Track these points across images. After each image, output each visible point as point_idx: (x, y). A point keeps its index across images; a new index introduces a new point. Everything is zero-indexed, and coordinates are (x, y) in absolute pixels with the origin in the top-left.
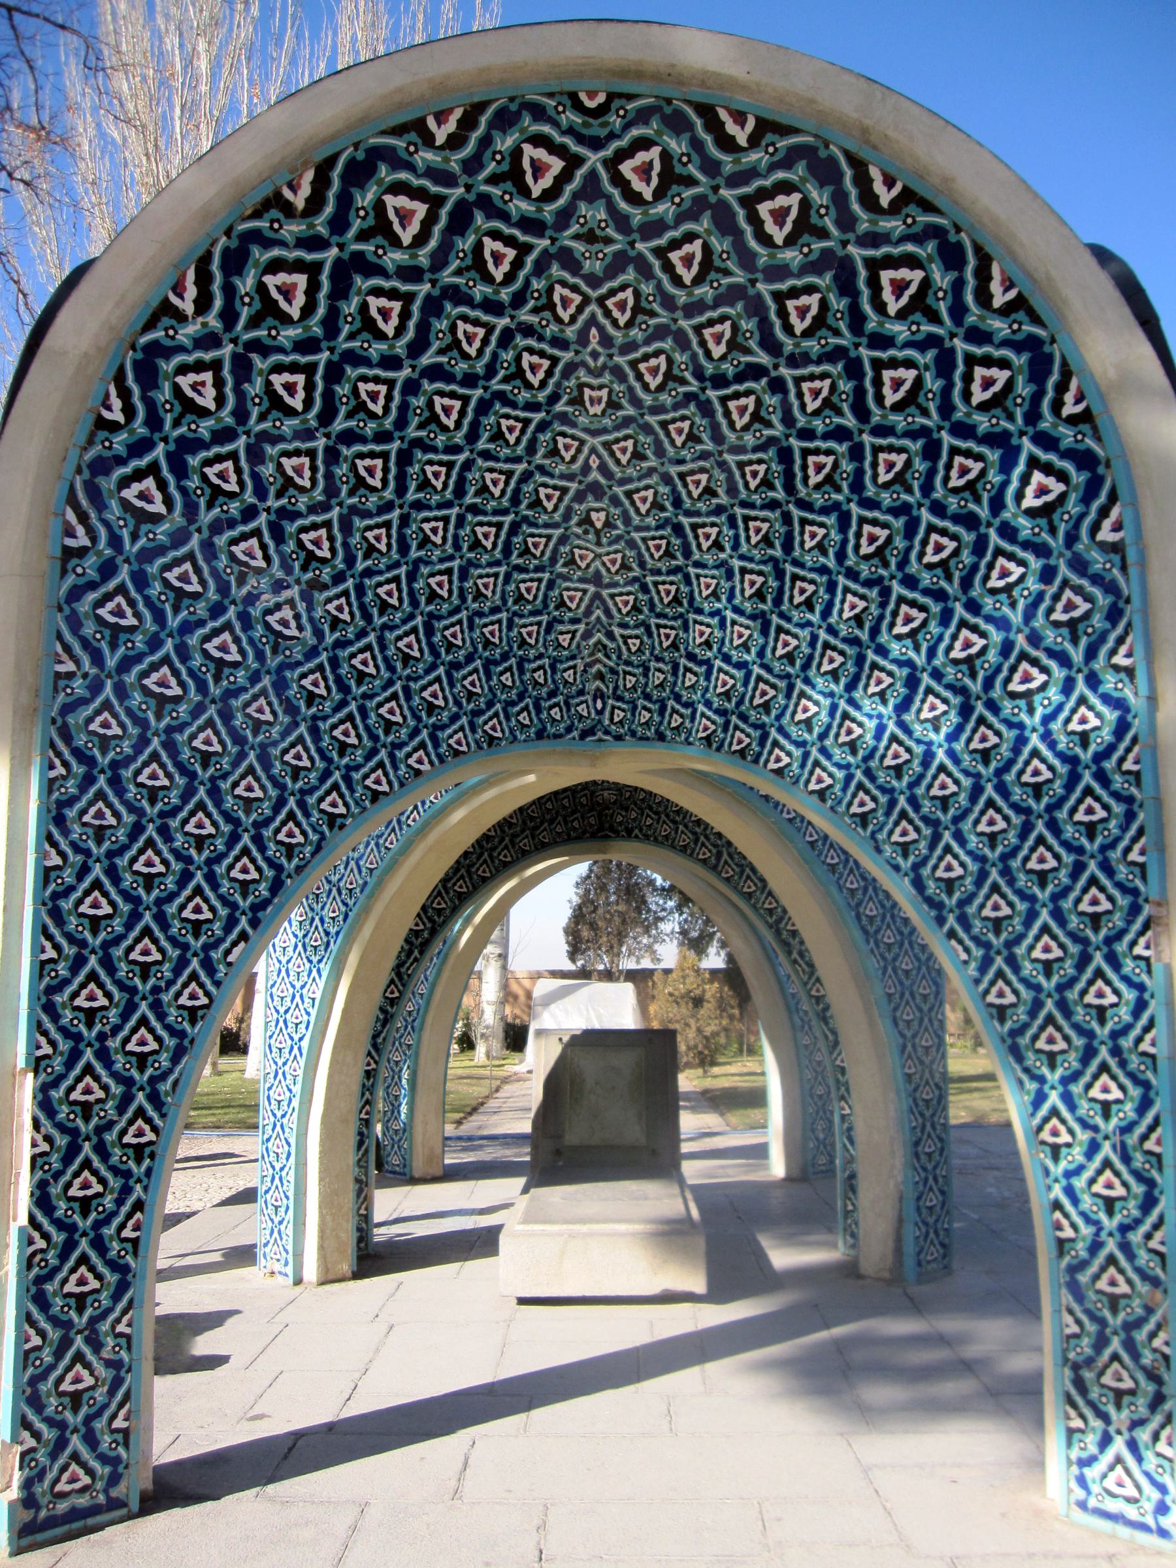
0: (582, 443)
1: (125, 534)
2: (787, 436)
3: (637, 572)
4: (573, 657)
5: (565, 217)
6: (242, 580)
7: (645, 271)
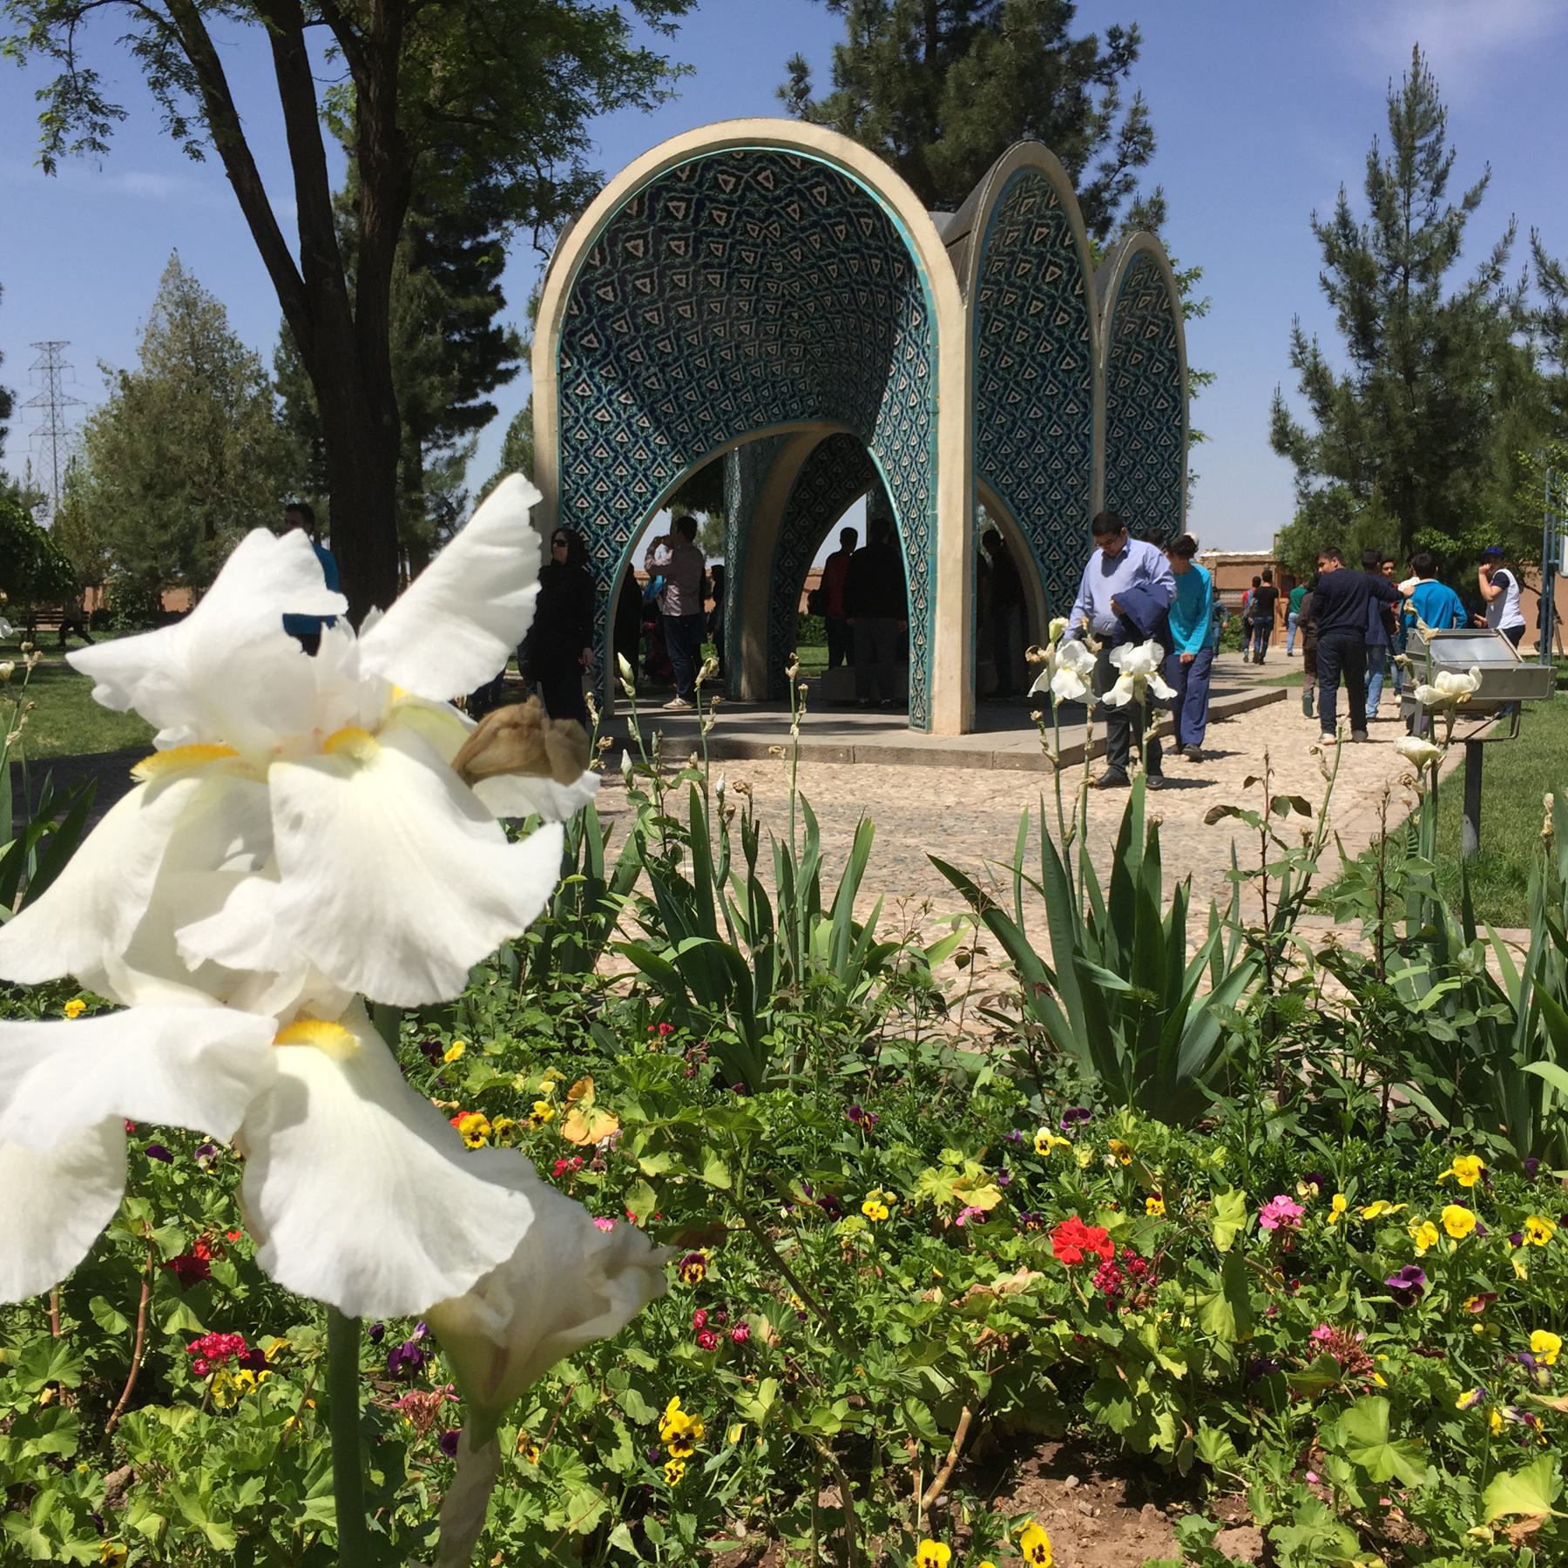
5: (742, 199)
6: (633, 369)
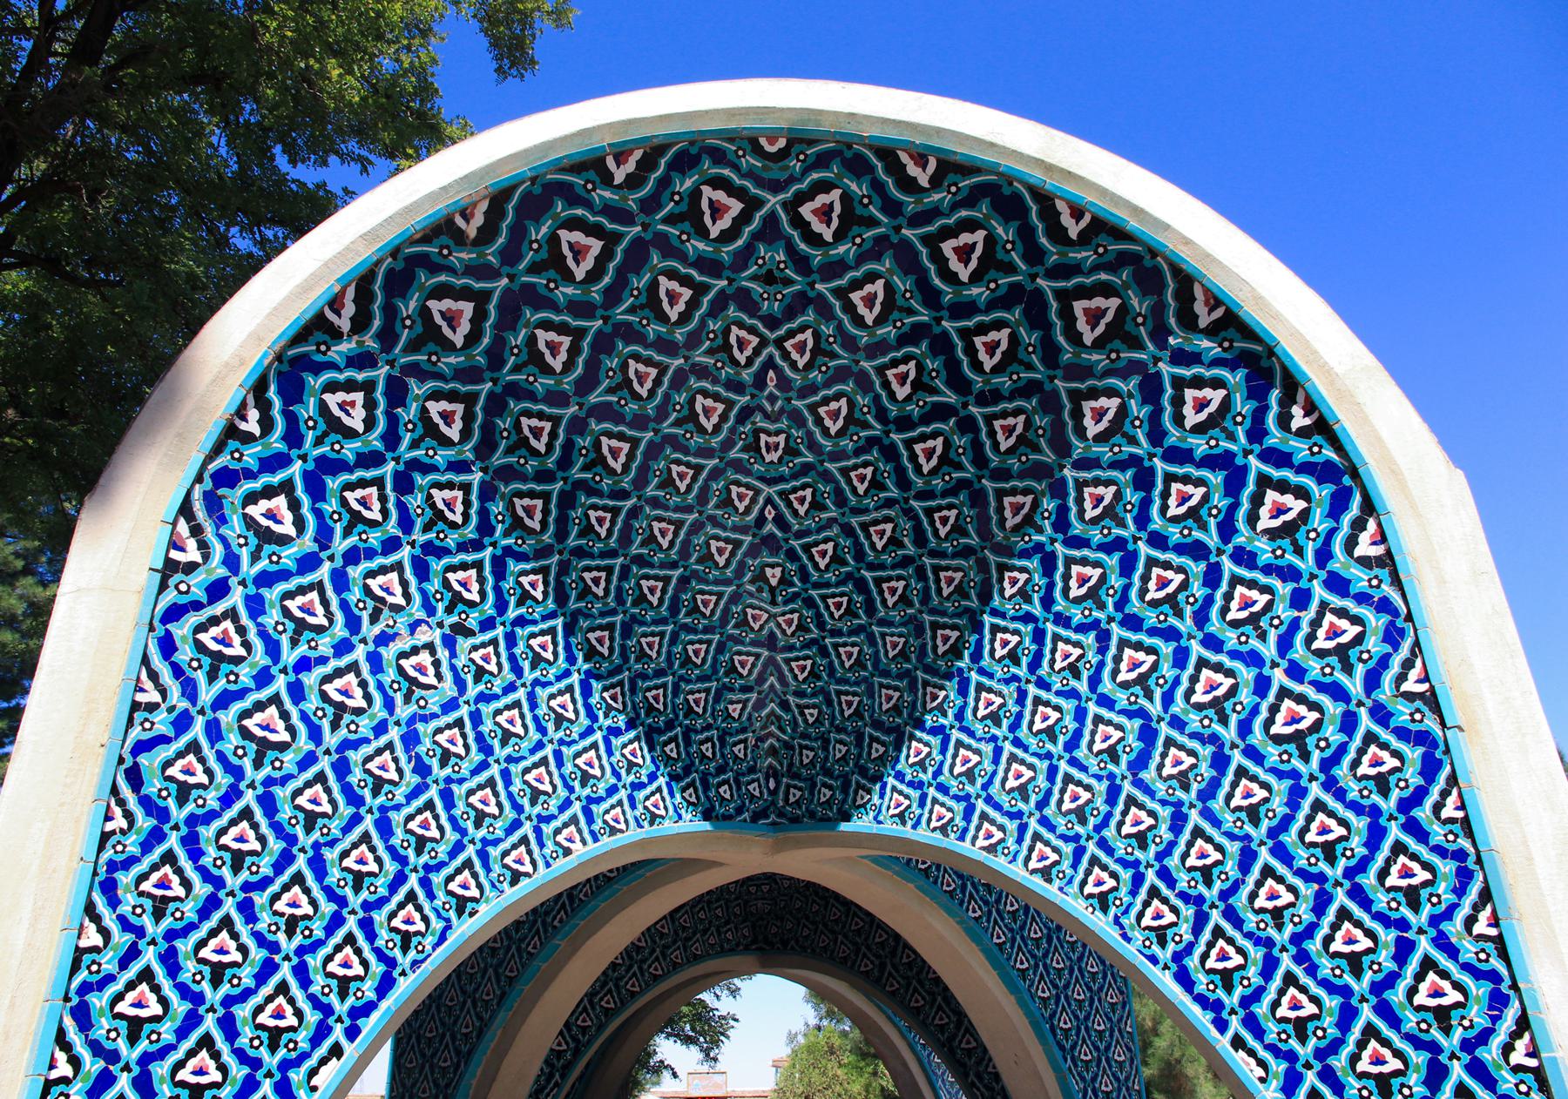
0: (757, 492)
1: (245, 555)
2: (980, 478)
3: (815, 633)
4: (744, 730)
6: (374, 619)
7: (825, 312)
